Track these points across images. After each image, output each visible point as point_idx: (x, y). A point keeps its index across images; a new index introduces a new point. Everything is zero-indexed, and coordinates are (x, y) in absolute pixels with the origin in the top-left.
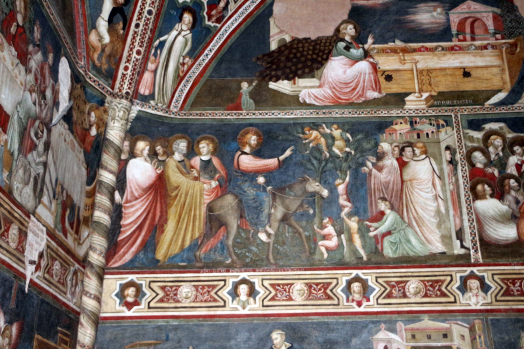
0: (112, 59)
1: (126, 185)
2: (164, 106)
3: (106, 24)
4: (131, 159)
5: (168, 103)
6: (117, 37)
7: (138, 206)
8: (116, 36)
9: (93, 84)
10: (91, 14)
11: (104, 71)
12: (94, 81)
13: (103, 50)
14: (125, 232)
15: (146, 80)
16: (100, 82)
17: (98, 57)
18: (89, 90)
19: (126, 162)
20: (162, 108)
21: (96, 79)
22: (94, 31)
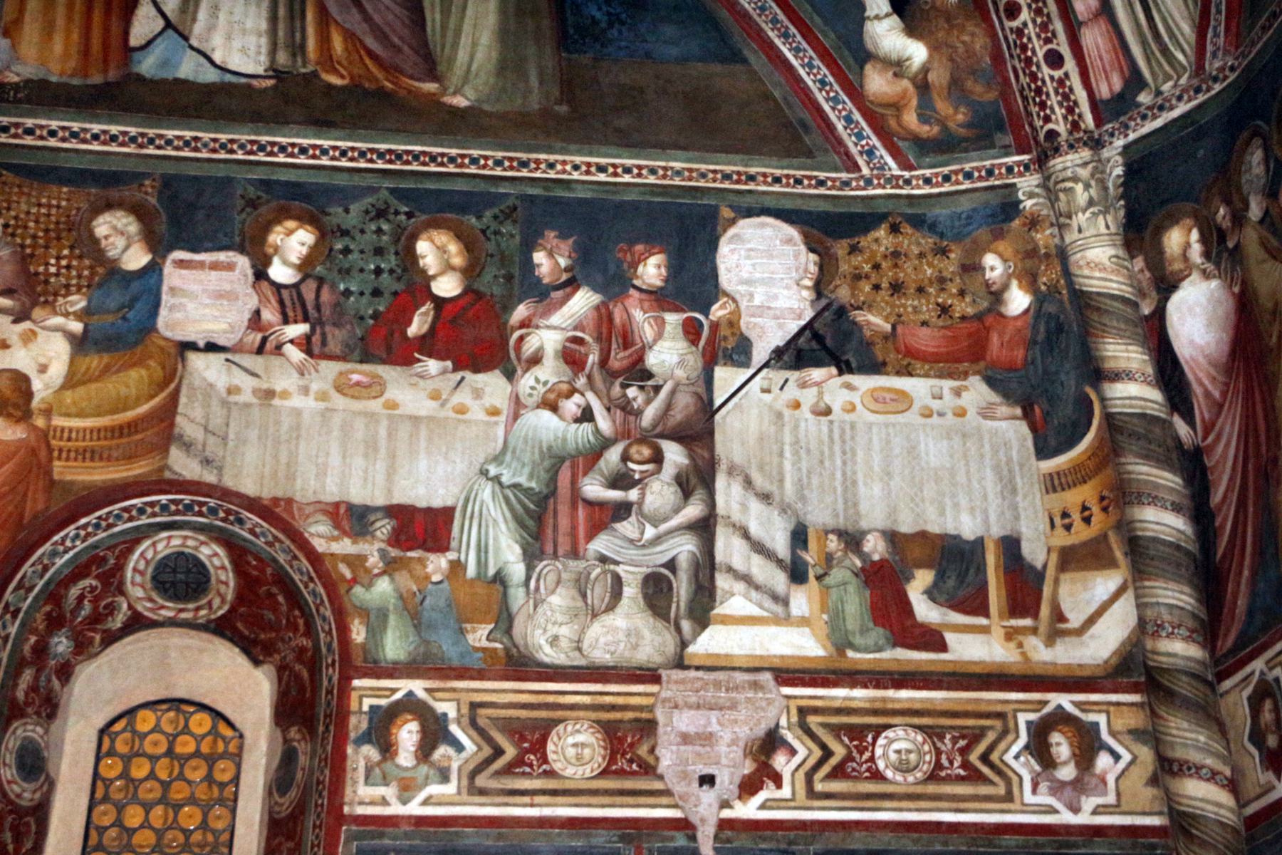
0: (969, 84)
1: (1188, 384)
2: (1183, 81)
3: (895, 17)
4: (1167, 299)
5: (1193, 59)
6: (948, 20)
7: (1227, 429)
8: (942, 23)
9: (947, 188)
10: (839, 38)
11: (962, 131)
12: (947, 178)
13: (922, 85)
14: (1223, 526)
15: (1094, 53)
16: (967, 167)
17: (919, 115)
18: (940, 212)
19: (1160, 315)
20: (1178, 93)
21: (946, 170)
22: (868, 68)
